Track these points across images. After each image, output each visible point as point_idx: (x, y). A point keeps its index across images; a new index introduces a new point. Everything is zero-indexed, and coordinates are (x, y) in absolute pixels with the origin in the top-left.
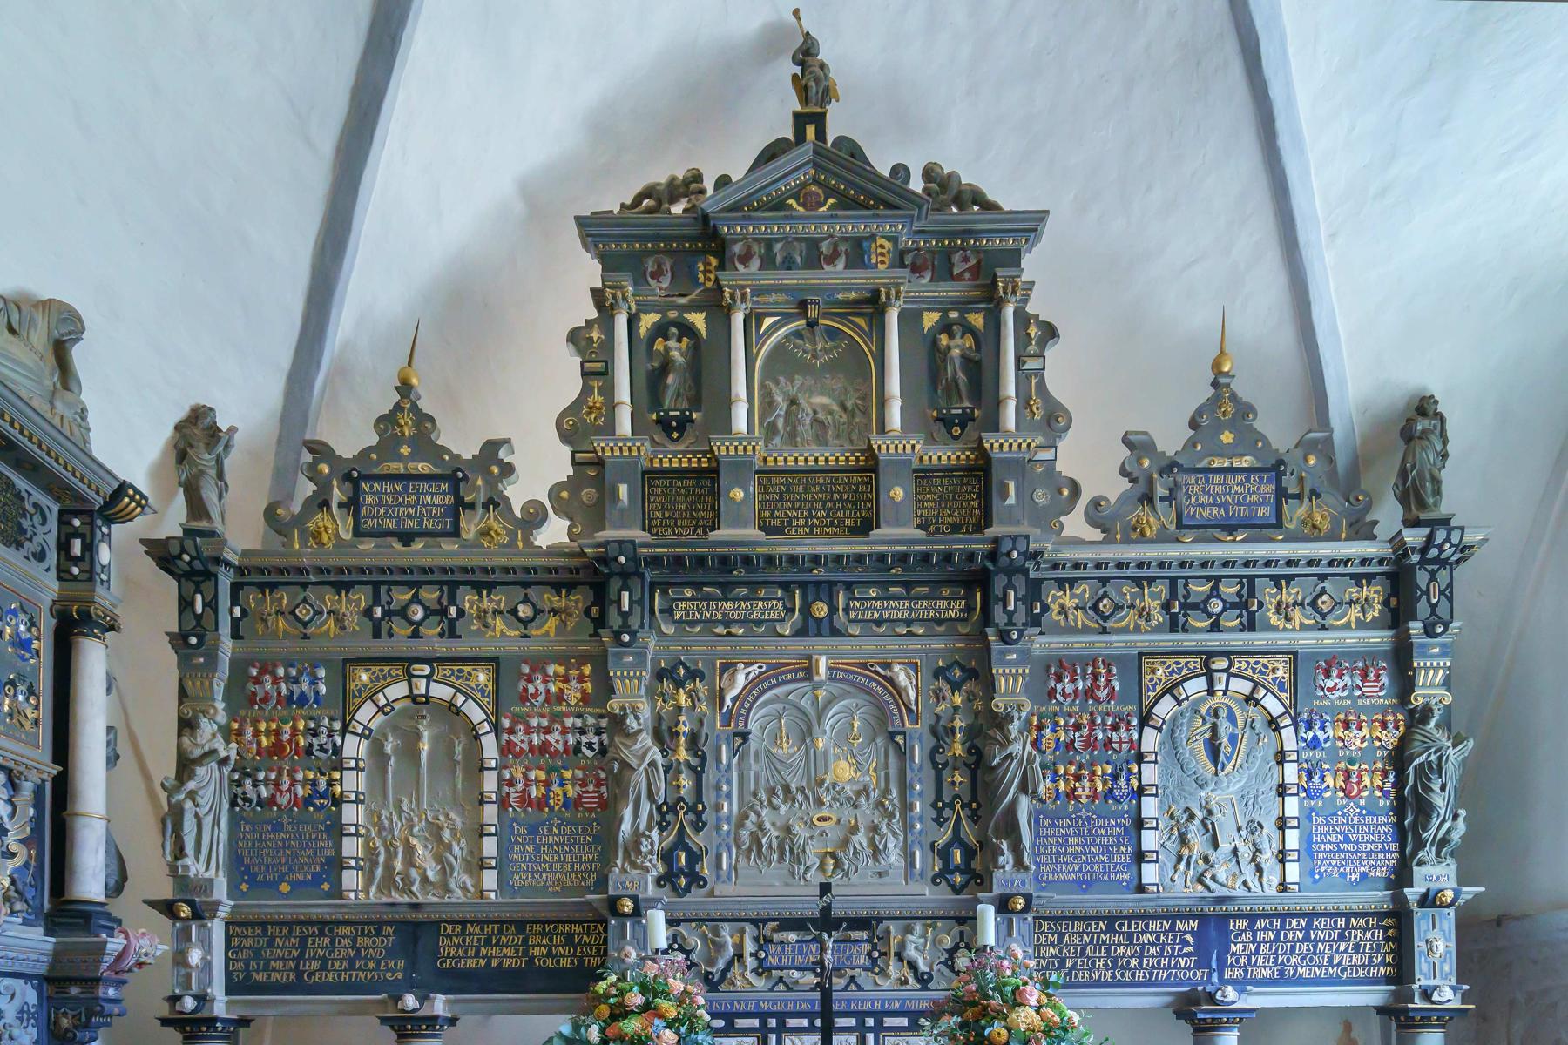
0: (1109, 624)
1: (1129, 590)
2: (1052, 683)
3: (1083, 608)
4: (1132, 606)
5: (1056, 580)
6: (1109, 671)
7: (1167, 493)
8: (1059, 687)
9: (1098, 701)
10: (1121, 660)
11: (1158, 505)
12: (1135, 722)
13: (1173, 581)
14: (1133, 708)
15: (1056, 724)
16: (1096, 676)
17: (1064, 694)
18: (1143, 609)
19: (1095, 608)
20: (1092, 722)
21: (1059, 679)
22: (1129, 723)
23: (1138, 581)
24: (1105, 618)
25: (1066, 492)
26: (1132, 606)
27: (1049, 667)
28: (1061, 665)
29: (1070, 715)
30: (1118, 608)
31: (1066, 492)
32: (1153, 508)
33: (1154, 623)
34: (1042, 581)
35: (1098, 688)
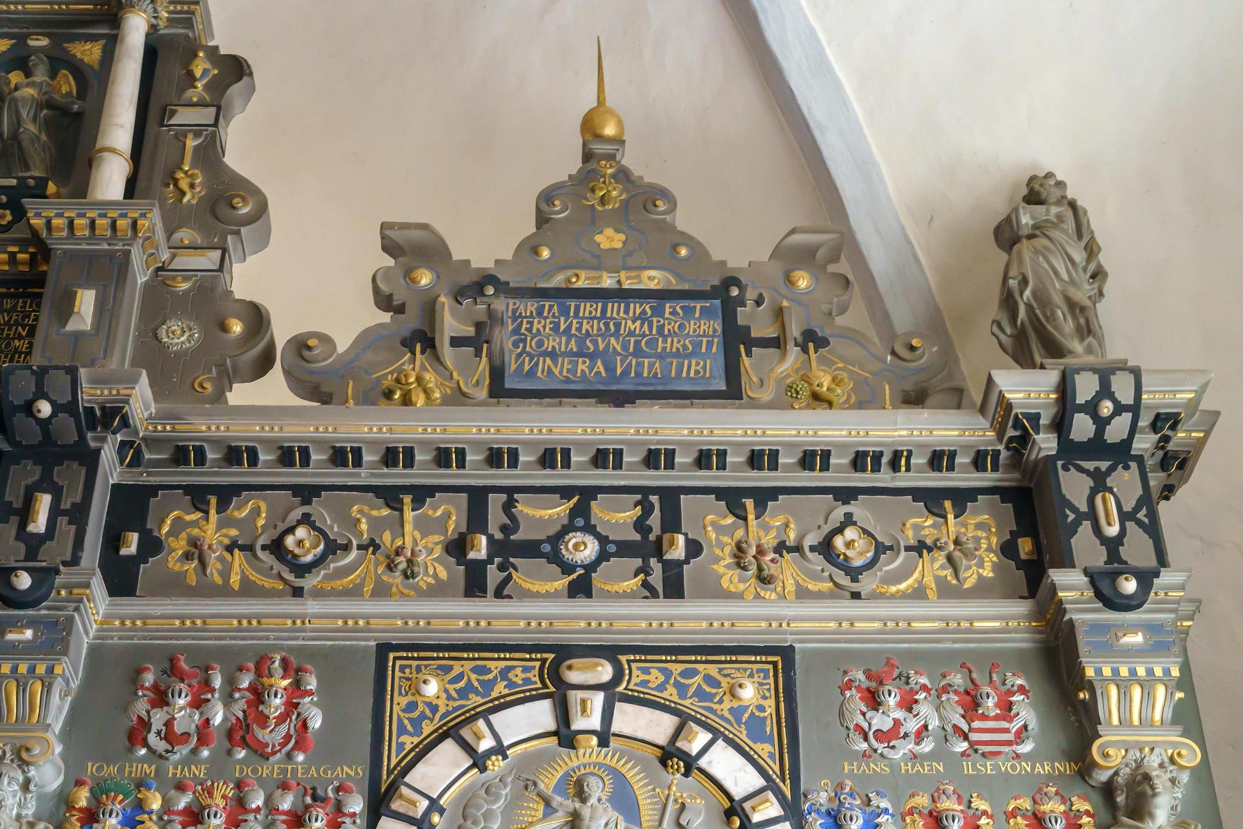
0: (310, 582)
1: (367, 515)
2: (141, 707)
3: (249, 548)
4: (373, 545)
5: (188, 489)
6: (297, 684)
7: (470, 331)
8: (158, 718)
9: (260, 752)
10: (332, 661)
11: (448, 353)
12: (356, 804)
13: (477, 497)
14: (355, 772)
15: (140, 806)
16: (258, 695)
17: (169, 735)
18: (398, 553)
19: (277, 547)
20: (240, 803)
21: (161, 698)
22: (339, 808)
23: (390, 496)
24: (302, 570)
25: (237, 328)
26: (373, 545)
27: (140, 671)
28: (172, 670)
29: (181, 787)
30: (334, 548)
31: (237, 328)
32: (438, 359)
33: (423, 580)
34: (153, 490)
35: (263, 720)
